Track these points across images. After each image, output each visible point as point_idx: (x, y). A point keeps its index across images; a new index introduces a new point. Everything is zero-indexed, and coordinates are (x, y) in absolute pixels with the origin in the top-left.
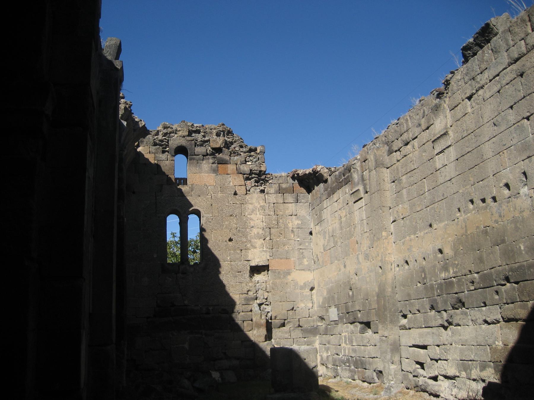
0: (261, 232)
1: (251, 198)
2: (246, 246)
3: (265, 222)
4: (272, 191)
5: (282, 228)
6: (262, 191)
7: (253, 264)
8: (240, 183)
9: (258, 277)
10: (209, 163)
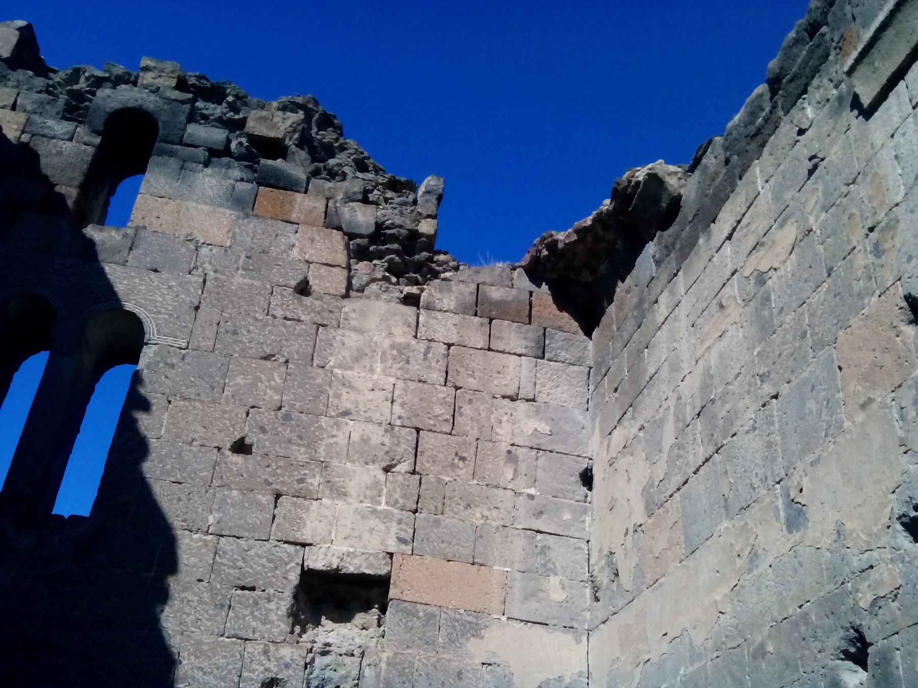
0: (377, 436)
1: (363, 314)
2: (301, 481)
3: (403, 405)
4: (449, 302)
5: (471, 439)
6: (411, 300)
7: (318, 561)
8: (327, 258)
9: (330, 632)
10: (226, 177)
